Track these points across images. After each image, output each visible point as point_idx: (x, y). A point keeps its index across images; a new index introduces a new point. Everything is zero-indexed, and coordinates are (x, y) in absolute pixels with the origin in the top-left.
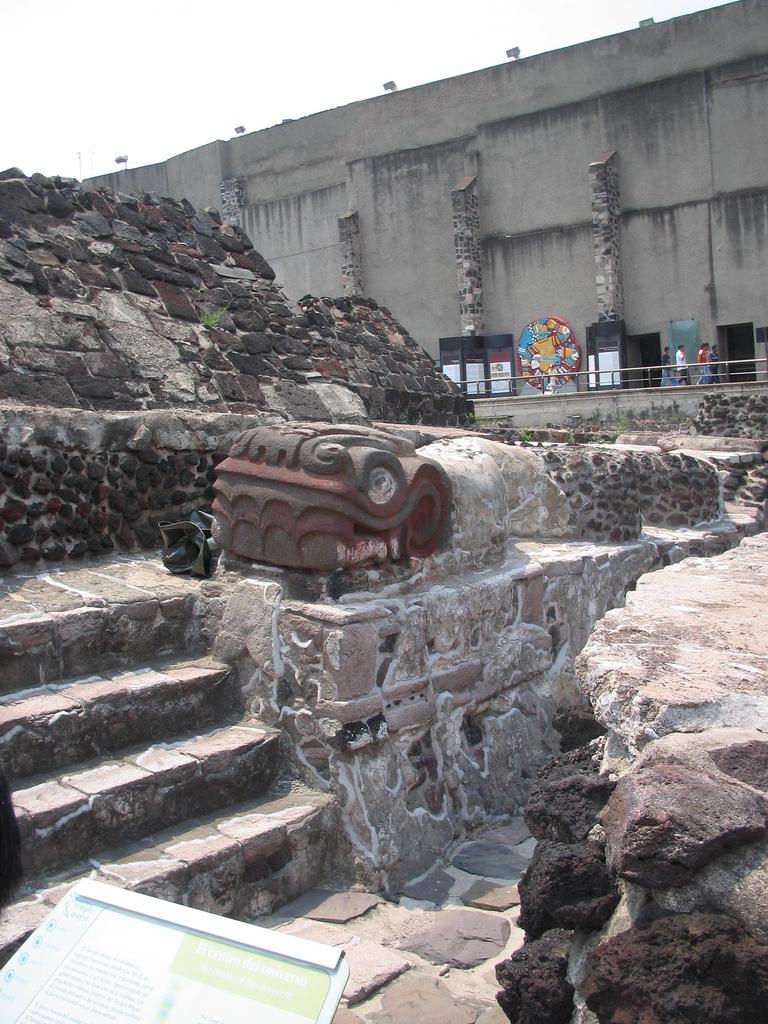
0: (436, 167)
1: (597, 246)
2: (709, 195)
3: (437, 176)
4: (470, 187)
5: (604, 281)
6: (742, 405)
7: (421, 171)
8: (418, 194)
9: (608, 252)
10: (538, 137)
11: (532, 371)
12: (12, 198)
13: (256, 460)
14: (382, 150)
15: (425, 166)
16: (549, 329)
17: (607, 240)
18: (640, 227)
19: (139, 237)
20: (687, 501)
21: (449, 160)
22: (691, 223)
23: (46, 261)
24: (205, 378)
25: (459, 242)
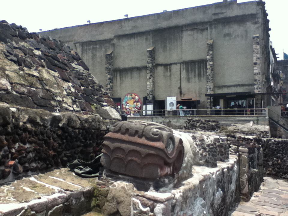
0: (101, 47)
1: (148, 74)
2: (181, 61)
3: (101, 50)
4: (111, 53)
5: (149, 83)
6: (198, 122)
7: (96, 48)
8: (95, 54)
9: (151, 76)
10: (133, 41)
11: (126, 109)
12: (6, 29)
13: (124, 134)
14: (85, 39)
15: (98, 46)
16: (132, 97)
17: (151, 72)
18: (160, 69)
19: (48, 50)
20: (222, 153)
21: (105, 45)
22: (175, 69)
23: (21, 54)
24: (74, 102)
25: (107, 70)
